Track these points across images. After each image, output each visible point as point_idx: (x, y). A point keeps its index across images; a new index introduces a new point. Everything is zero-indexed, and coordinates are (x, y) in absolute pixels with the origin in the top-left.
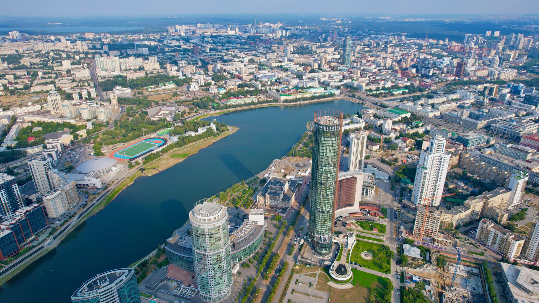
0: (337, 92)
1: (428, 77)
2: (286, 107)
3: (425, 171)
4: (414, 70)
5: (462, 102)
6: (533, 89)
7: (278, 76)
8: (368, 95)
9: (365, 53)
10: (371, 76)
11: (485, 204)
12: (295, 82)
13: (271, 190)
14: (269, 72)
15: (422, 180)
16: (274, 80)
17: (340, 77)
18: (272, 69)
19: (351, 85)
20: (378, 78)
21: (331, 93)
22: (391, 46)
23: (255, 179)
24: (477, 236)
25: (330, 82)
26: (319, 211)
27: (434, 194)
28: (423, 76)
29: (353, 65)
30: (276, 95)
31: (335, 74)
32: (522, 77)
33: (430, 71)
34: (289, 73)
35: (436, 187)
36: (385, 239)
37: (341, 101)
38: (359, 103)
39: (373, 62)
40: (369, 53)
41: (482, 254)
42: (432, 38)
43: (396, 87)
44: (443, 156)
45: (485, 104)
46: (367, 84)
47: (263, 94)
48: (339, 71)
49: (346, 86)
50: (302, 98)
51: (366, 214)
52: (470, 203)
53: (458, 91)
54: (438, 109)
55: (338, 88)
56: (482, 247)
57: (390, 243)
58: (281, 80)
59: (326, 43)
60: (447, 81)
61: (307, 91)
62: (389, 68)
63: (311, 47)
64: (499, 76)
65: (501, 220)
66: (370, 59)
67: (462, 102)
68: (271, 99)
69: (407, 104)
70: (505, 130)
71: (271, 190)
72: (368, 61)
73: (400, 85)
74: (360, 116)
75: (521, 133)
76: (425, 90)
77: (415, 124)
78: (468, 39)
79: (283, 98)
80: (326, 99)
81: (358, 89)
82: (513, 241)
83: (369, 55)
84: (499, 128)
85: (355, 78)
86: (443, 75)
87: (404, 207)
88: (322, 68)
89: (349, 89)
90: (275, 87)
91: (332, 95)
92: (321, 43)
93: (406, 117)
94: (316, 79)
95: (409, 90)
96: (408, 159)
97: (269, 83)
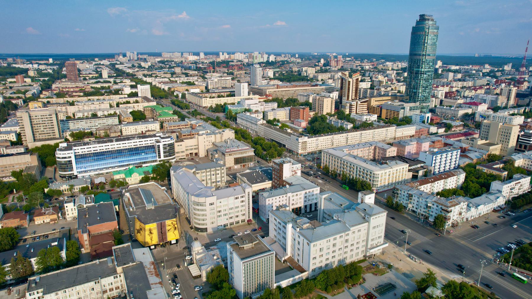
63: (306, 71)
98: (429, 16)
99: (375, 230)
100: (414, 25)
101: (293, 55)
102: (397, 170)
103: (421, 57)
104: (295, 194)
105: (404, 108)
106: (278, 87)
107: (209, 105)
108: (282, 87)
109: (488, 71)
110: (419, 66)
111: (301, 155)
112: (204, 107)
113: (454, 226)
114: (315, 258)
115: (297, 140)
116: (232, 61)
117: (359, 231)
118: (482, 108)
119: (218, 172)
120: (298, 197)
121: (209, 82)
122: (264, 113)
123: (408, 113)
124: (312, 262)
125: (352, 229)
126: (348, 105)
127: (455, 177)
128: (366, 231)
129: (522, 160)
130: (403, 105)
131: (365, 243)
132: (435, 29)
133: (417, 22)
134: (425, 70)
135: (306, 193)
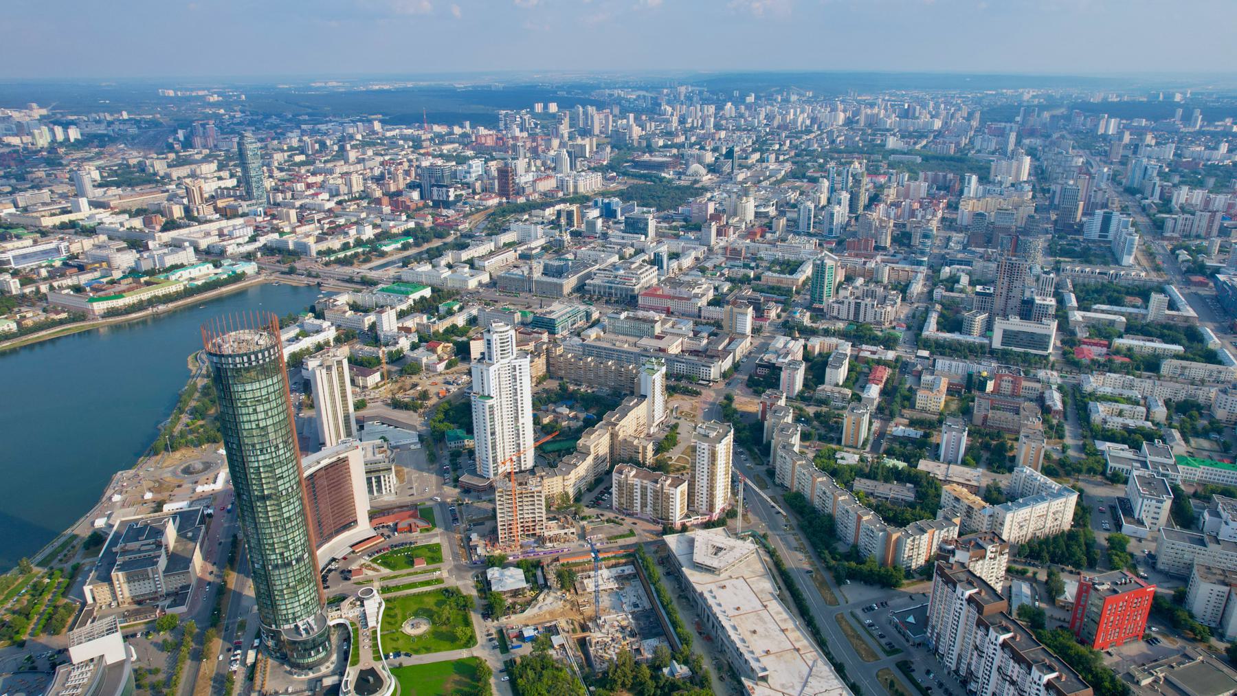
0: (250, 268)
1: (447, 204)
2: (116, 328)
3: (490, 402)
4: (415, 195)
5: (525, 247)
6: (633, 205)
7: (68, 249)
8: (327, 264)
9: (297, 169)
10: (324, 218)
11: (613, 436)
12: (126, 260)
13: (127, 558)
14: (35, 242)
15: (488, 424)
16: (58, 264)
17: (250, 231)
18: (44, 233)
20: (342, 221)
21: (234, 272)
22: (353, 147)
23: (64, 546)
24: (615, 504)
25: (224, 247)
26: (276, 567)
27: (519, 445)
28: (437, 204)
29: (274, 198)
30: (78, 302)
31: (234, 226)
32: (613, 186)
33: (448, 191)
34: (103, 238)
35: (518, 430)
36: (445, 574)
37: (264, 287)
38: (309, 286)
39: (322, 186)
40: (308, 167)
41: (632, 533)
42: (438, 123)
43: (385, 236)
44: (517, 363)
45: (566, 243)
46: (320, 239)
47: (33, 305)
48: (242, 216)
49: (269, 250)
50: (156, 297)
51: (391, 534)
52: (588, 443)
53: (513, 226)
54: (483, 269)
55: (249, 257)
56: (629, 520)
57: (460, 578)
58: (82, 260)
59: (191, 152)
60: (487, 208)
61: (167, 278)
62: (360, 195)
63: (153, 166)
64: (576, 187)
65: (644, 458)
66: (311, 180)
67: (525, 247)
68: (64, 315)
69: (419, 270)
70: (610, 288)
71: (127, 558)
72: (309, 186)
73: (395, 231)
74: (320, 316)
75: (636, 287)
76: (449, 234)
77: (446, 308)
78: (506, 120)
79: (100, 307)
80: (224, 290)
81: (300, 251)
82: (672, 490)
83: (308, 171)
84: (599, 286)
85: (287, 229)
86: (477, 197)
87: (467, 490)
89: (278, 257)
90: (69, 282)
91: (237, 278)
92: (177, 153)
93: (423, 298)
94: (187, 244)
95: (416, 238)
96: (450, 387)
97: (44, 273)
123: (246, 210)
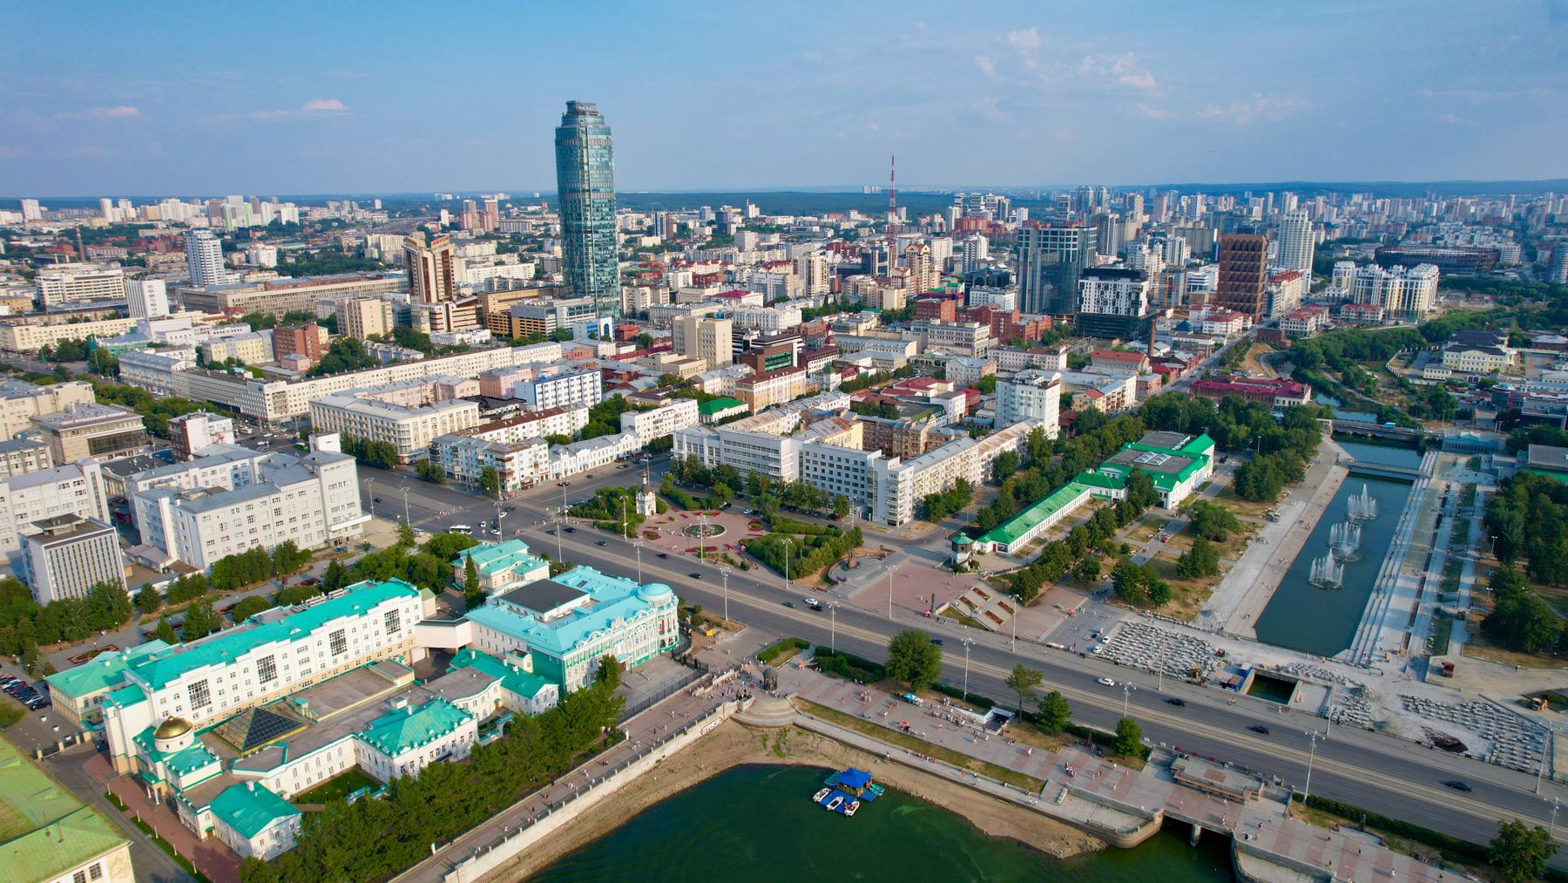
9: (652, 257)
17: (589, 389)
19: (743, 464)
25: (500, 454)
31: (535, 366)
40: (674, 255)
63: (378, 246)
88: (426, 328)
89: (736, 527)
94: (330, 443)
98: (589, 105)
99: (335, 491)
100: (559, 124)
101: (366, 204)
102: (451, 416)
103: (580, 196)
104: (209, 470)
105: (554, 311)
106: (267, 286)
107: (39, 346)
108: (282, 286)
109: (851, 225)
110: (579, 215)
111: (274, 423)
112: (25, 352)
113: (525, 486)
114: (212, 542)
115: (261, 390)
116: (151, 227)
117: (301, 493)
118: (756, 299)
119: (28, 459)
120: (218, 476)
121: (45, 285)
122: (199, 350)
123: (565, 321)
124: (206, 550)
125: (283, 489)
126: (426, 313)
127: (564, 415)
128: (319, 494)
129: (718, 380)
130: (552, 304)
131: (321, 517)
132: (602, 133)
133: (564, 118)
134: (594, 223)
135: (236, 468)
